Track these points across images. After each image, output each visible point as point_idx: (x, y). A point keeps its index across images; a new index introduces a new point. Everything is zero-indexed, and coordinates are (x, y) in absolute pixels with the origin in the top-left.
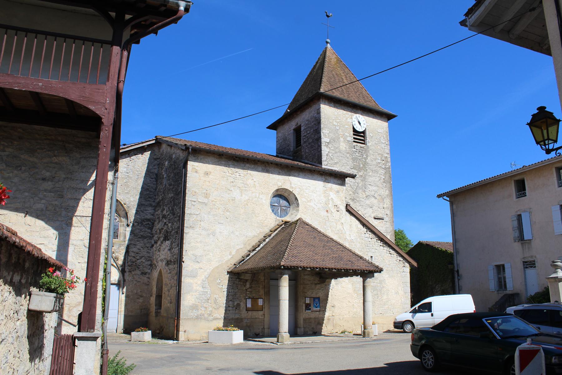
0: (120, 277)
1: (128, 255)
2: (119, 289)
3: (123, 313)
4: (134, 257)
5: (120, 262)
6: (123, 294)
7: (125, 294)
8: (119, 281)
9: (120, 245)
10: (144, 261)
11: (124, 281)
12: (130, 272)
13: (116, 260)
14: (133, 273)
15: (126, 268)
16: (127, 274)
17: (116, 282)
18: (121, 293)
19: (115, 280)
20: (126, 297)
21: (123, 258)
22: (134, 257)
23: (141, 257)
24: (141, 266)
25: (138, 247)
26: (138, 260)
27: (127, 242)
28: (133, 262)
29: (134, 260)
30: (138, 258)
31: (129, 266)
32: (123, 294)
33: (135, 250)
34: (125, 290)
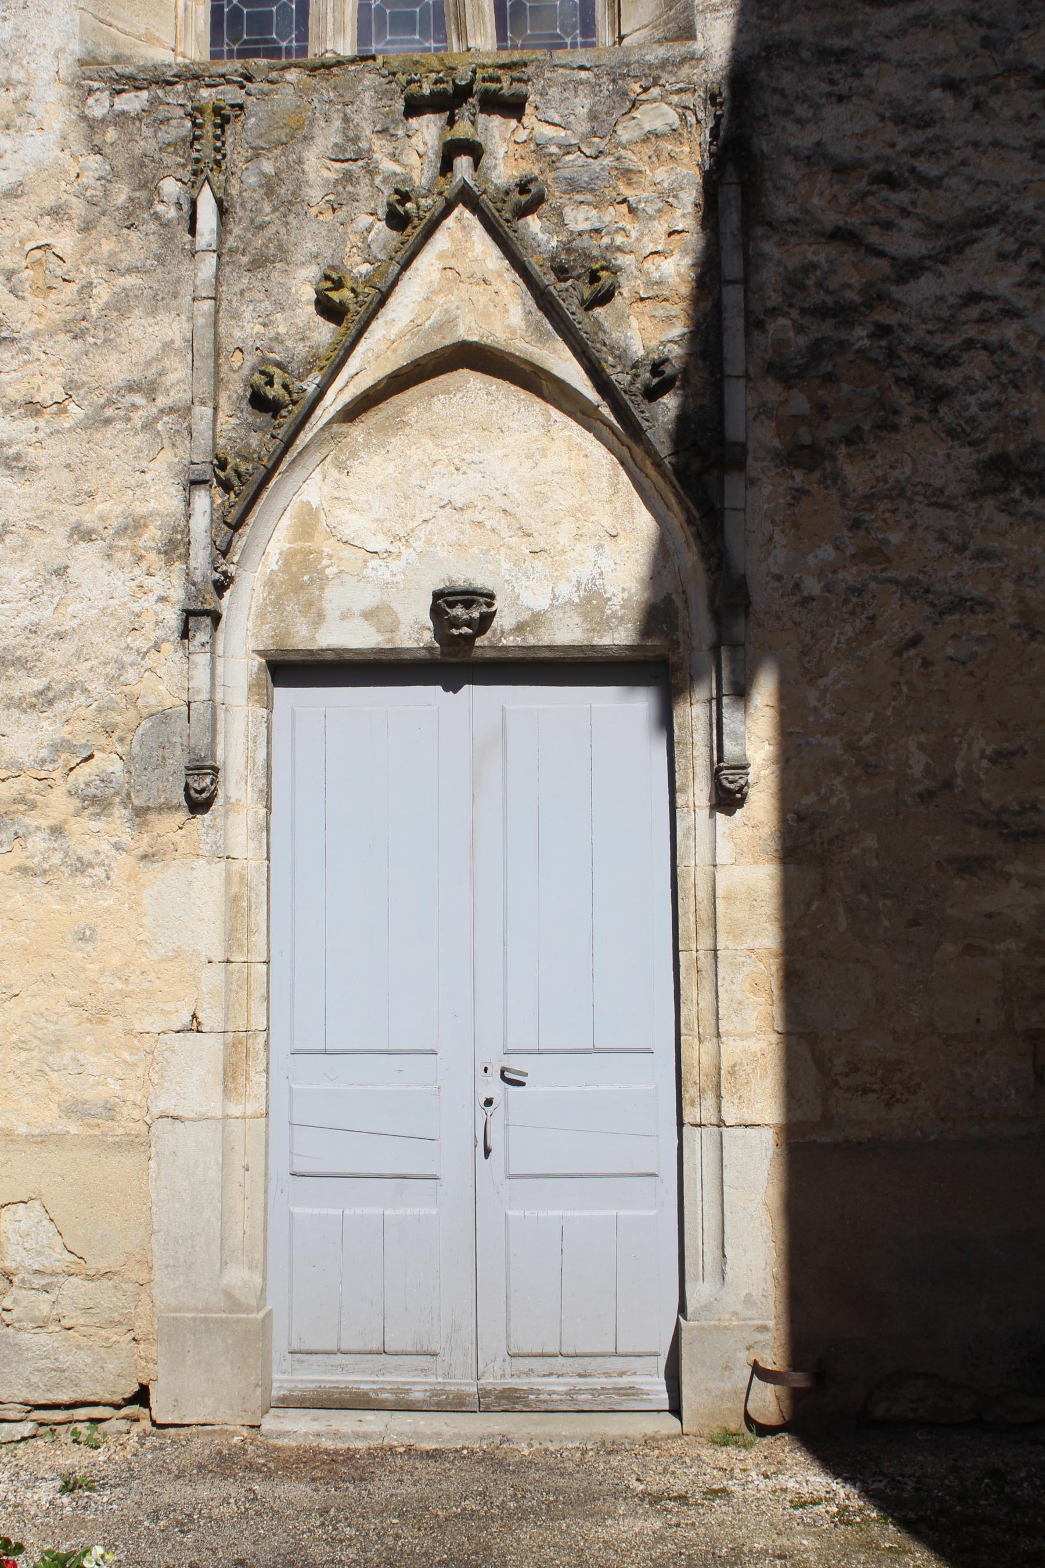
0: (663, 554)
1: (753, 214)
2: (666, 722)
3: (759, 1102)
4: (842, 236)
5: (648, 327)
6: (727, 799)
7: (761, 803)
8: (659, 615)
9: (624, 87)
10: (1004, 283)
11: (730, 597)
12: (803, 455)
13: (570, 296)
14: (856, 475)
15: (738, 400)
16: (757, 499)
17: (620, 636)
18: (698, 792)
19: (592, 603)
20: (801, 845)
21: (676, 269)
22: (842, 236)
23: (956, 237)
24: (975, 366)
25: (890, 84)
26: (909, 270)
27: (716, 36)
28: (842, 313)
29: (850, 276)
30: (907, 242)
31: (780, 371)
32: (727, 799)
33: (844, 127)
34: (755, 736)
